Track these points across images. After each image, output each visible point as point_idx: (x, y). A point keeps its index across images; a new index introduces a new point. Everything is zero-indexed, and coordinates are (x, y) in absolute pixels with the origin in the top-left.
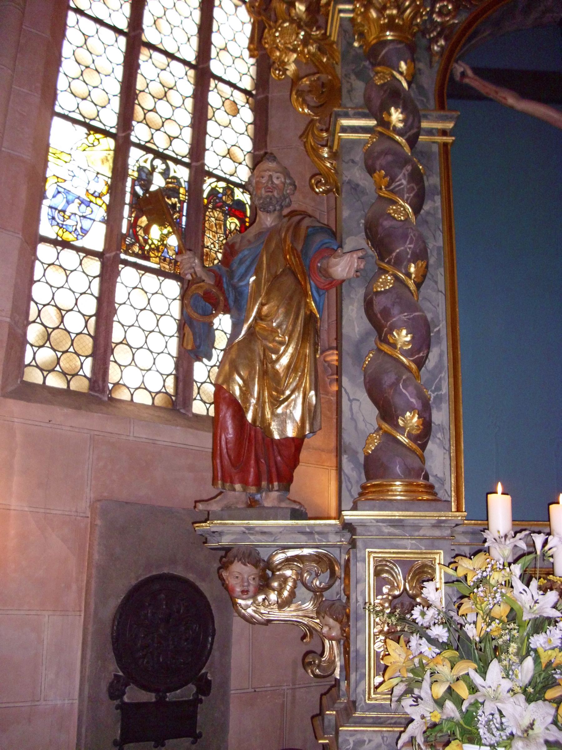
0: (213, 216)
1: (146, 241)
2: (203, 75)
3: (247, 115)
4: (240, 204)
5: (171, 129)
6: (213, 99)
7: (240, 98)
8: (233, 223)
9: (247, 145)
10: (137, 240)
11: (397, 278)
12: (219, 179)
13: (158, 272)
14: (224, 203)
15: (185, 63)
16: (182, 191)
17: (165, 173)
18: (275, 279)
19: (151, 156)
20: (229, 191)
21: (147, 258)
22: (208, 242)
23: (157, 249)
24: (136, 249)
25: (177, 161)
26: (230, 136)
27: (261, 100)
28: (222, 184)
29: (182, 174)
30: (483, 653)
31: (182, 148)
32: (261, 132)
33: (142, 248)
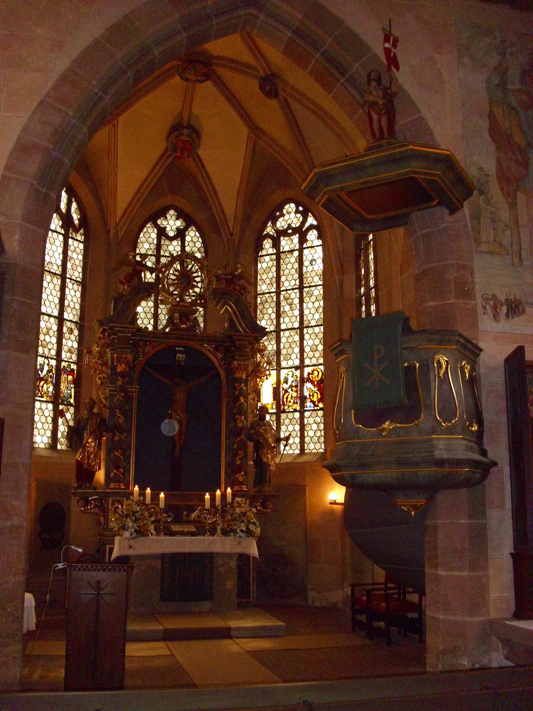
0: (64, 377)
1: (42, 391)
2: (61, 320)
3: (76, 332)
4: (73, 370)
5: (50, 346)
6: (65, 330)
7: (73, 326)
8: (70, 378)
9: (75, 345)
10: (40, 391)
11: (120, 437)
12: (66, 361)
13: (46, 402)
14: (67, 371)
15: (54, 317)
16: (54, 370)
17: (48, 364)
18: (91, 432)
19: (43, 358)
20: (69, 366)
21: (42, 397)
22: (62, 387)
23: (46, 393)
24: (39, 394)
25: (52, 359)
26: (70, 343)
27: (81, 325)
28: (67, 363)
29: (53, 363)
30: (127, 516)
31: (53, 352)
32: (81, 340)
33: (41, 394)
